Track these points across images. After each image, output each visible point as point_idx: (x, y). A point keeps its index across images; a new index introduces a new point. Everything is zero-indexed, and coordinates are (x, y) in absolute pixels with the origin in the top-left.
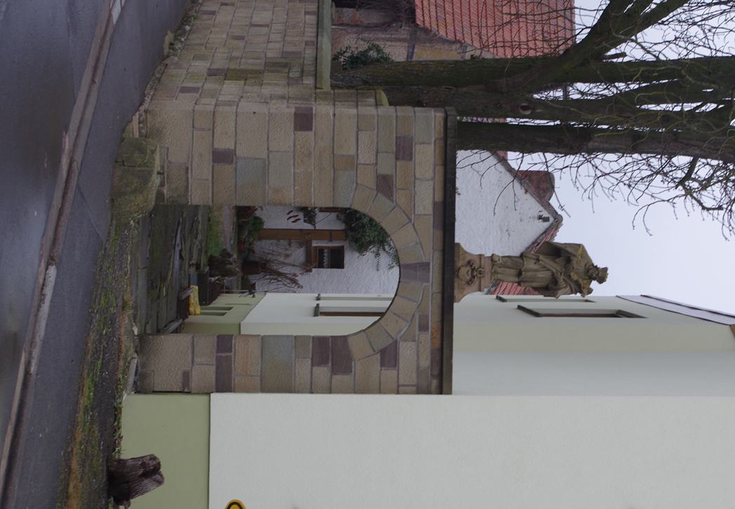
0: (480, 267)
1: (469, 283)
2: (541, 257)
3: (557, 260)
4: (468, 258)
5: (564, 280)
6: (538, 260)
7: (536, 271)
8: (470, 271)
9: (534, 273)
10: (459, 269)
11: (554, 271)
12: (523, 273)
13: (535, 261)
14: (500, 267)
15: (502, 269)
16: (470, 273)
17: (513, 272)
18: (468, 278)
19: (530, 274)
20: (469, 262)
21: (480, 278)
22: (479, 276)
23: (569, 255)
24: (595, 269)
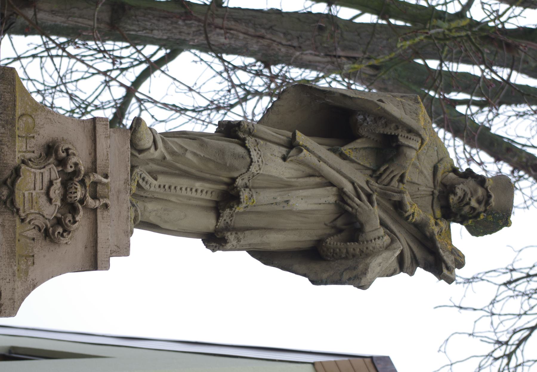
0: (94, 170)
1: (53, 232)
2: (301, 138)
3: (346, 149)
4: (46, 133)
5: (383, 224)
6: (292, 144)
7: (286, 186)
8: (57, 184)
9: (279, 196)
10: (17, 172)
11: (348, 188)
12: (244, 195)
13: (284, 150)
14: (154, 175)
15: (162, 180)
16: (56, 191)
17: (205, 191)
18: (51, 211)
19: (265, 197)
20: (50, 149)
21: (95, 210)
22: (90, 201)
23: (390, 131)
24: (471, 182)
